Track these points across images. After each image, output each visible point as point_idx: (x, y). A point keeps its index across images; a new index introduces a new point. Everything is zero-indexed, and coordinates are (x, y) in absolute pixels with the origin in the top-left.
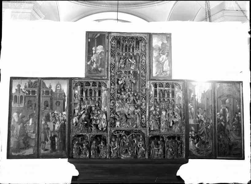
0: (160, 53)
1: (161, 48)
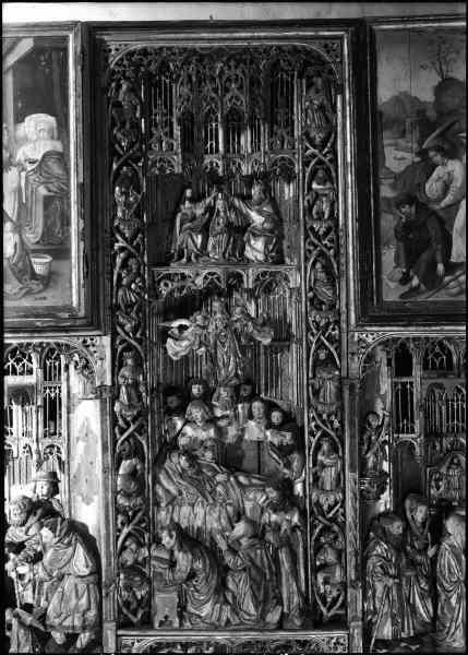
1: (431, 114)
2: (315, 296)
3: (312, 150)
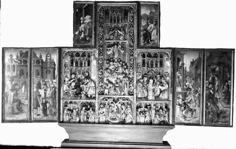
0: (148, 23)
1: (149, 17)
3: (130, 22)
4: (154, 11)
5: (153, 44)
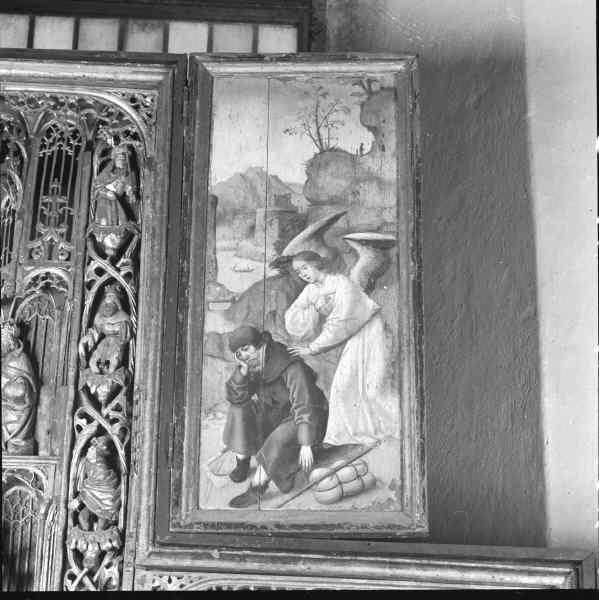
0: (290, 259)
1: (300, 203)
2: (82, 506)
3: (97, 263)
4: (352, 137)
5: (343, 497)
